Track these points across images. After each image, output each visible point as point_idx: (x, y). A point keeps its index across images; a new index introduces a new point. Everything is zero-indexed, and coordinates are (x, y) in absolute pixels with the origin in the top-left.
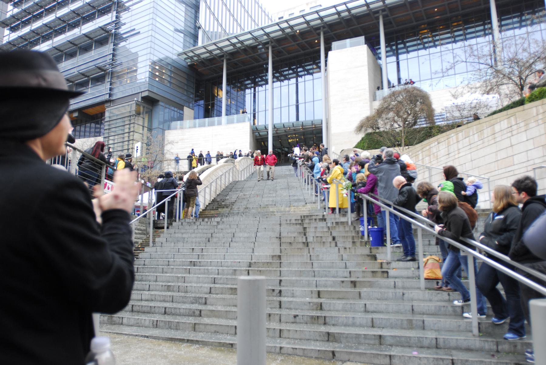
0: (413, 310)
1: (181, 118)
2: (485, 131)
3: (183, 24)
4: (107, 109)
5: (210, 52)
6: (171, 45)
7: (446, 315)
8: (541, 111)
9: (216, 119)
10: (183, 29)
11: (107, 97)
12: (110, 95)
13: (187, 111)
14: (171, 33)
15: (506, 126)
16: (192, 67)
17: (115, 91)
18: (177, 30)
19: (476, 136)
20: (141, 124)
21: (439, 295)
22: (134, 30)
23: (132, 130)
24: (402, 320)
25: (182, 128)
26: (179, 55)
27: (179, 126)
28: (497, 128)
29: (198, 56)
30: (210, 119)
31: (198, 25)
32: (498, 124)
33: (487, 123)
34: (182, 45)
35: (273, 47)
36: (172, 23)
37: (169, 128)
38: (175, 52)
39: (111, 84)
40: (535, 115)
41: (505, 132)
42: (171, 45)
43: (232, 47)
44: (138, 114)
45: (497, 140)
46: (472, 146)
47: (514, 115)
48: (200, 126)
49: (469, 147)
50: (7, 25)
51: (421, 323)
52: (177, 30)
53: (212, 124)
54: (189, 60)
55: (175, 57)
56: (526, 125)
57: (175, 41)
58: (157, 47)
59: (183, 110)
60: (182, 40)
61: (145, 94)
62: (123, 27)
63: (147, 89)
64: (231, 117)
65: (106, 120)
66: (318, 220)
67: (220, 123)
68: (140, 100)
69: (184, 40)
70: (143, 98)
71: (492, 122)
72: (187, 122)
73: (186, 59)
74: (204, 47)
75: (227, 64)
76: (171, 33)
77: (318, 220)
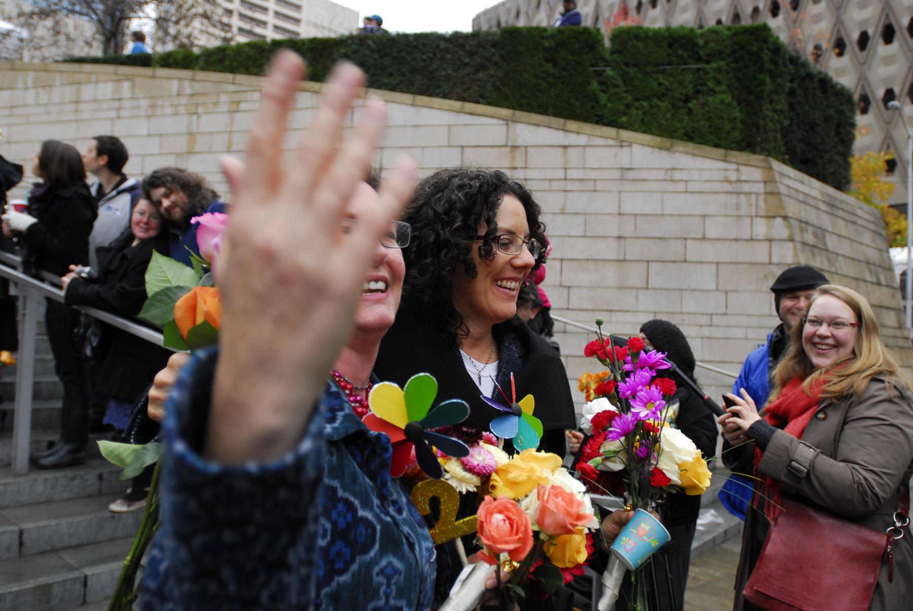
0: (21, 544)
2: (56, 91)
7: (115, 539)
8: (188, 90)
15: (109, 96)
19: (31, 93)
21: (76, 482)
24: (17, 594)
28: (87, 92)
32: (93, 86)
33: (65, 75)
40: (174, 93)
41: (104, 105)
45: (84, 116)
46: (16, 111)
47: (131, 78)
49: (7, 112)
51: (78, 587)
56: (154, 106)
71: (78, 77)
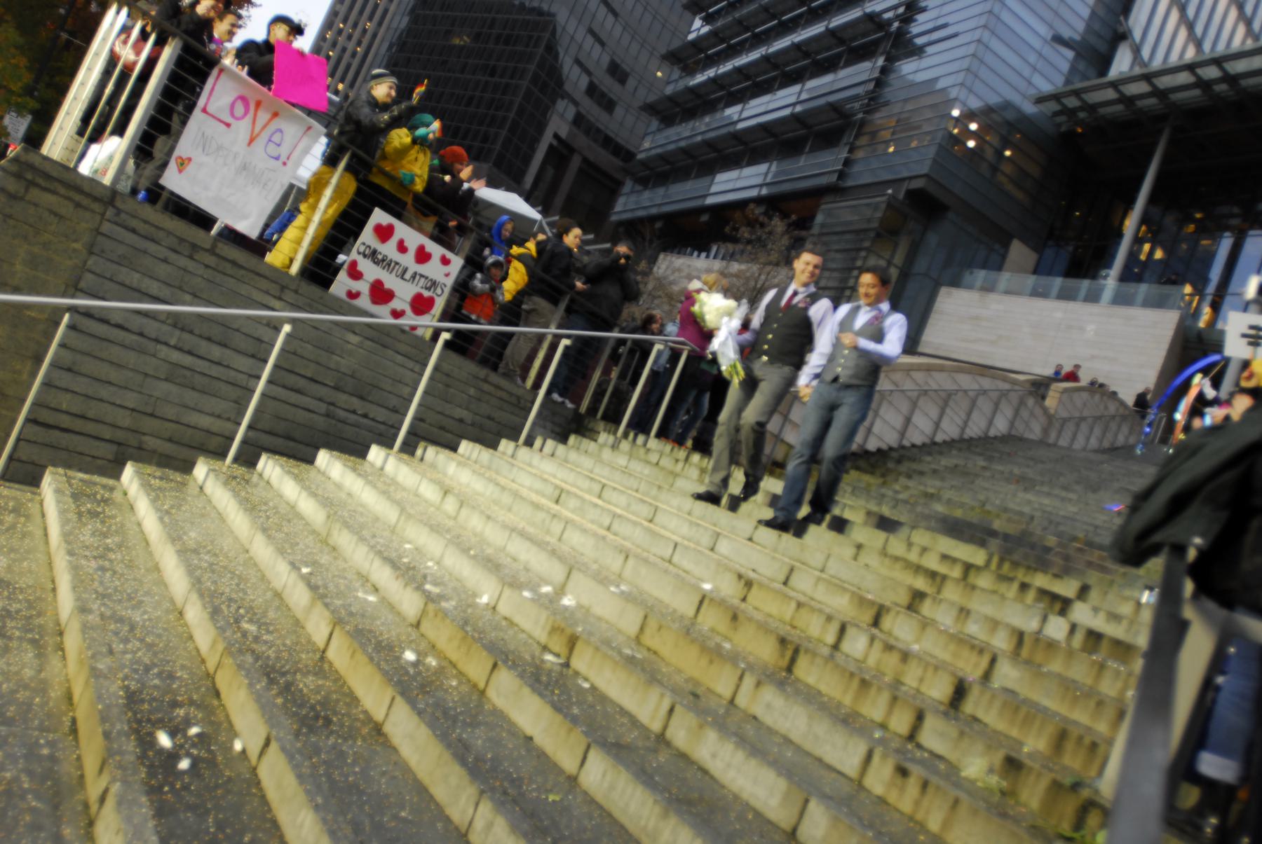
1: (996, 263)
3: (1080, 26)
4: (823, 207)
5: (1128, 101)
6: (1026, 72)
9: (1085, 284)
10: (1077, 37)
11: (834, 178)
12: (842, 175)
13: (1019, 251)
14: (1037, 43)
16: (1068, 139)
17: (856, 169)
18: (1058, 39)
20: (887, 257)
22: (945, 26)
23: (859, 263)
25: (988, 288)
26: (1040, 100)
27: (979, 283)
29: (1092, 108)
31: (1121, 30)
34: (1059, 81)
36: (1048, 15)
37: (956, 283)
38: (1032, 92)
39: (851, 151)
42: (1026, 72)
43: (1196, 92)
44: (887, 232)
48: (1036, 293)
50: (701, 10)
52: (1058, 39)
53: (1066, 295)
54: (1062, 119)
55: (1029, 108)
57: (1040, 65)
58: (984, 73)
59: (1006, 246)
60: (1065, 67)
61: (918, 184)
62: (921, 18)
63: (925, 170)
64: (1131, 287)
65: (816, 230)
66: (1031, 596)
67: (1093, 298)
68: (901, 196)
69: (1073, 69)
70: (911, 194)
72: (1005, 278)
73: (1056, 114)
74: (1114, 85)
75: (1172, 143)
76: (1037, 43)
77: (1031, 596)
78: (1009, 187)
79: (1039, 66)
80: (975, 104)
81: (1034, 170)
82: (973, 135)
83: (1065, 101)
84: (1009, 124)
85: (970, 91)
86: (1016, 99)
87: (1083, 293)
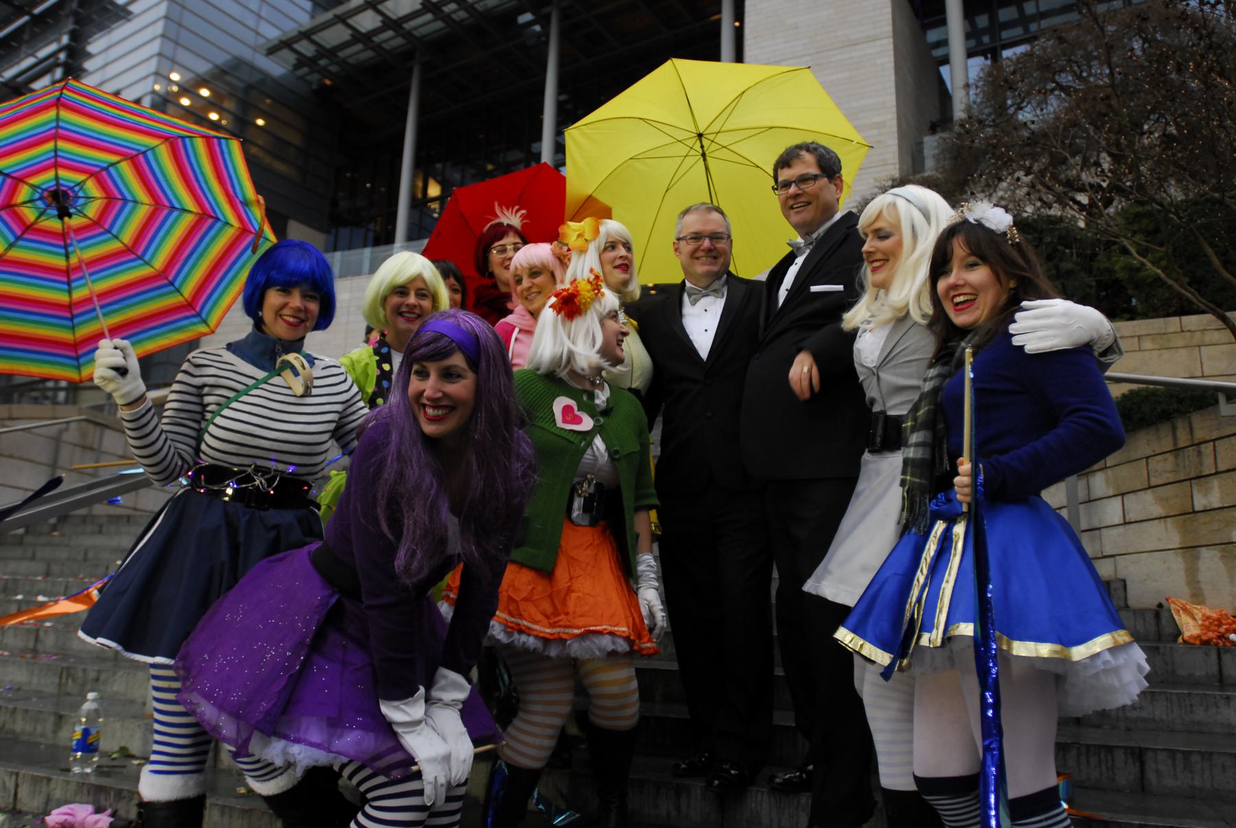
6: (251, 21)
26: (272, 51)
29: (331, 53)
30: (347, 253)
35: (564, 18)
38: (261, 41)
42: (251, 21)
58: (189, 20)
78: (268, 160)
79: (263, 14)
80: (203, 68)
81: (295, 139)
82: (211, 104)
83: (296, 46)
84: (250, 87)
85: (177, 43)
86: (247, 54)
87: (366, 266)
